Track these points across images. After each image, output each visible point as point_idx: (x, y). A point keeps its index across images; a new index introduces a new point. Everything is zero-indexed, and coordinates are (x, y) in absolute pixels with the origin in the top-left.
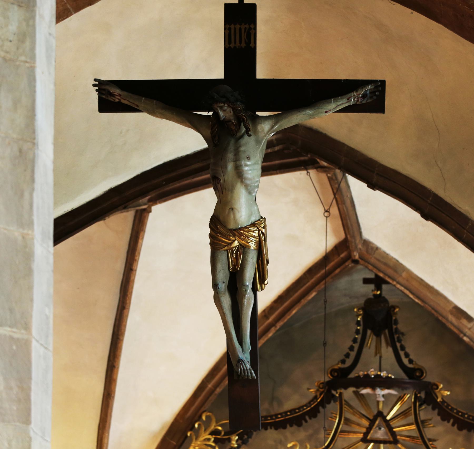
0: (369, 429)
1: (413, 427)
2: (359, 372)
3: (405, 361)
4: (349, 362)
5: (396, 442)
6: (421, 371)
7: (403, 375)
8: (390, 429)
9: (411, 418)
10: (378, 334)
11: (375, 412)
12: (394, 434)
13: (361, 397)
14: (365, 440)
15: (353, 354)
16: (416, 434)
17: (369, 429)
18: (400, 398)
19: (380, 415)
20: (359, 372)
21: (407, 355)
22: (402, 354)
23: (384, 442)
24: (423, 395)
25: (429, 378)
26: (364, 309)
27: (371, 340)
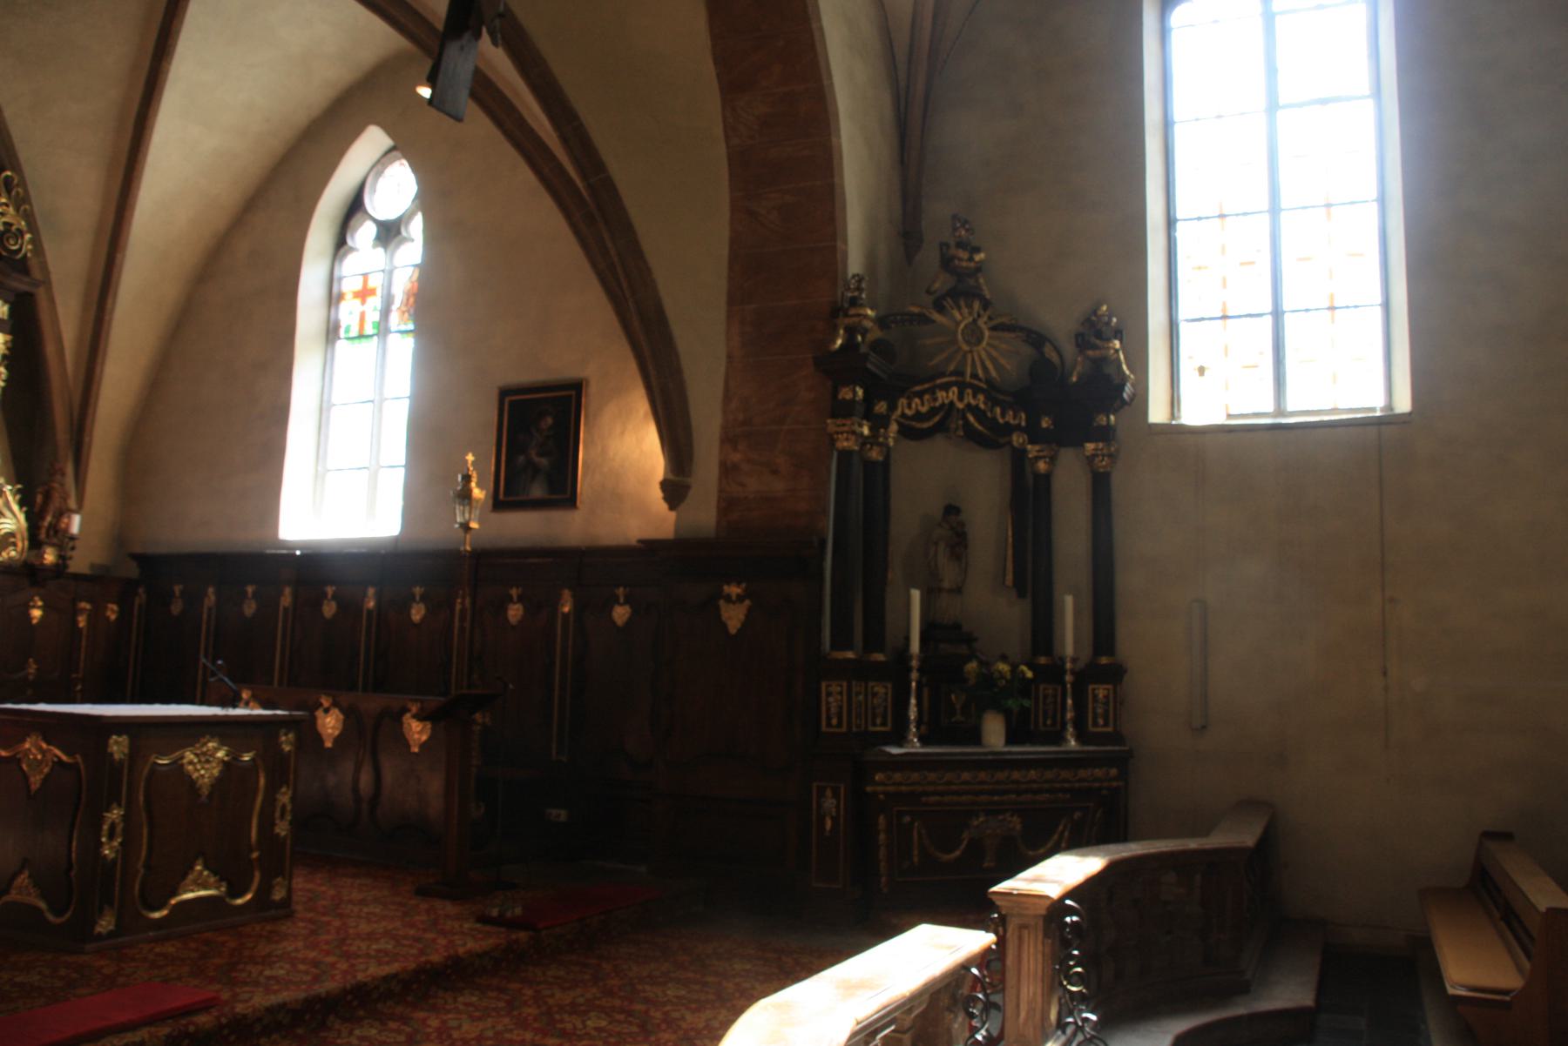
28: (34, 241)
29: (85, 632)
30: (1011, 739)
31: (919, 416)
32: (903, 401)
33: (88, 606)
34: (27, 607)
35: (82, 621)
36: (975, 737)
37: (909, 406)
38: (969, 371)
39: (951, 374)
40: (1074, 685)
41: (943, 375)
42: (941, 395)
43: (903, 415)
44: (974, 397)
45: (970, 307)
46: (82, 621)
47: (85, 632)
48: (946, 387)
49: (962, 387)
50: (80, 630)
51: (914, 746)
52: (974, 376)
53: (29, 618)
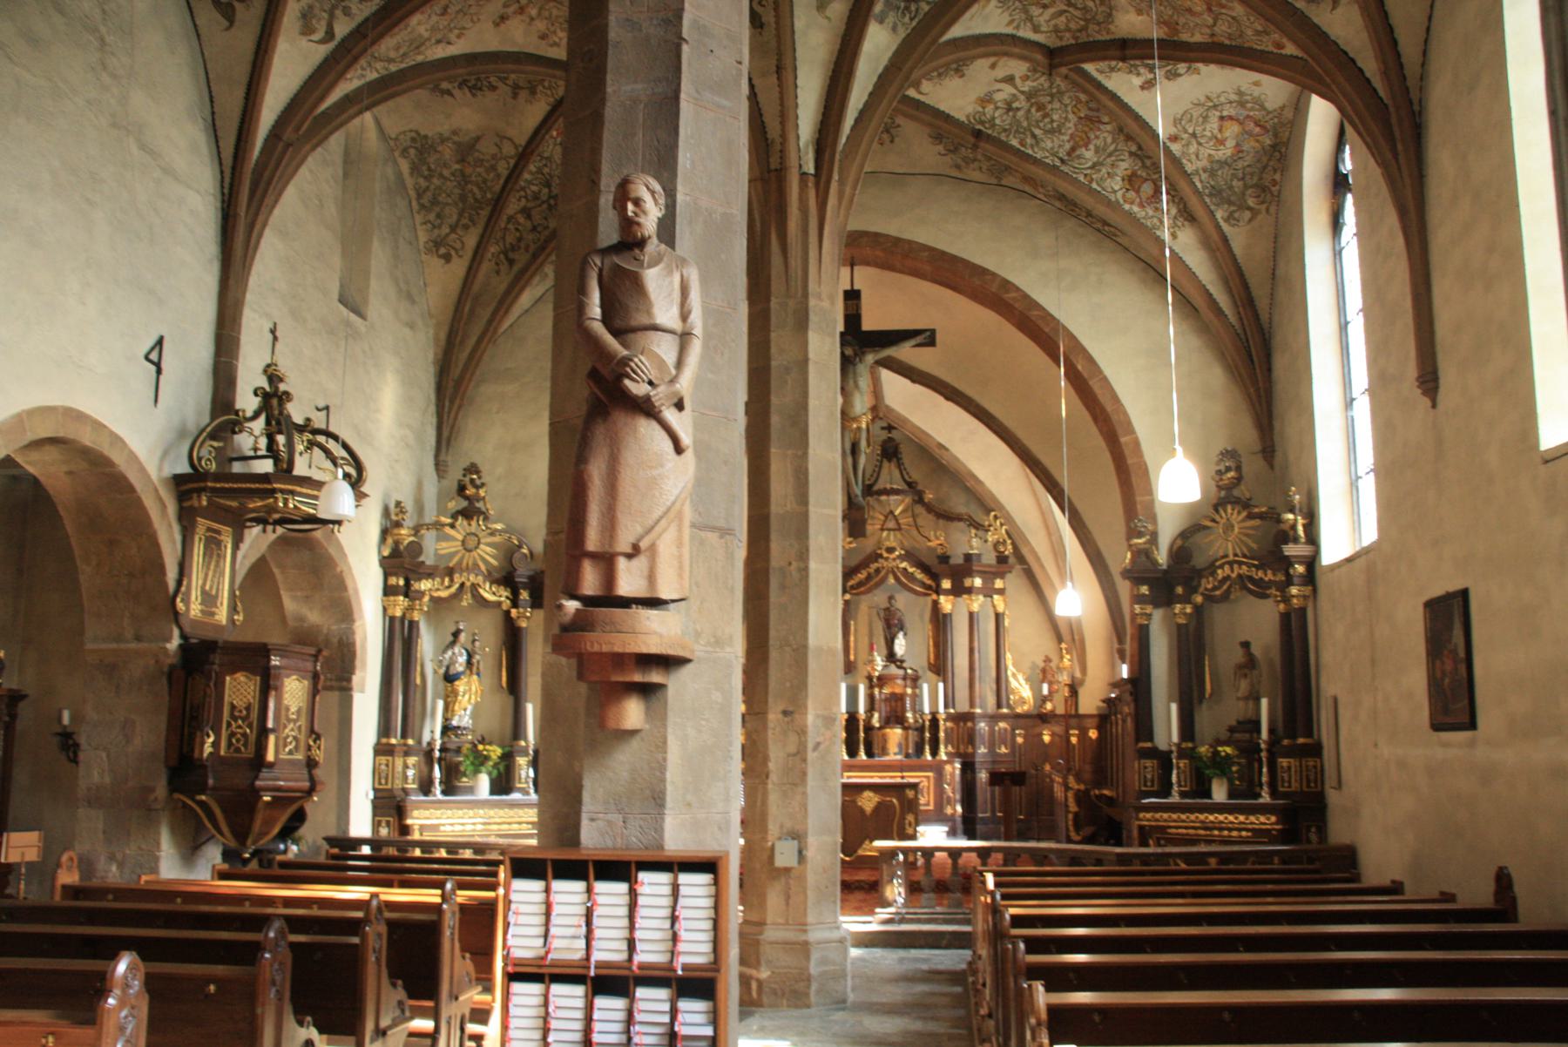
0: (885, 521)
1: (911, 519)
2: (879, 486)
3: (906, 477)
4: (873, 479)
5: (899, 529)
6: (916, 483)
7: (905, 487)
8: (897, 520)
9: (910, 513)
10: (890, 461)
11: (888, 510)
12: (898, 524)
13: (879, 501)
14: (882, 530)
15: (875, 475)
16: (912, 523)
17: (885, 521)
18: (903, 501)
19: (892, 512)
20: (879, 486)
21: (908, 474)
22: (904, 473)
23: (894, 530)
24: (916, 498)
25: (920, 487)
26: (882, 446)
27: (886, 464)
28: (1013, 544)
29: (1077, 748)
30: (1231, 795)
31: (1215, 588)
32: (1204, 581)
33: (1077, 732)
34: (1041, 734)
35: (1074, 740)
36: (1208, 795)
37: (1208, 582)
38: (1231, 553)
39: (1223, 557)
40: (1268, 759)
41: (1217, 560)
42: (1219, 571)
43: (1206, 589)
44: (1240, 568)
45: (1225, 511)
46: (1074, 740)
47: (1077, 748)
48: (1221, 567)
49: (1231, 564)
50: (1074, 745)
51: (1175, 798)
52: (1236, 555)
53: (1042, 740)
